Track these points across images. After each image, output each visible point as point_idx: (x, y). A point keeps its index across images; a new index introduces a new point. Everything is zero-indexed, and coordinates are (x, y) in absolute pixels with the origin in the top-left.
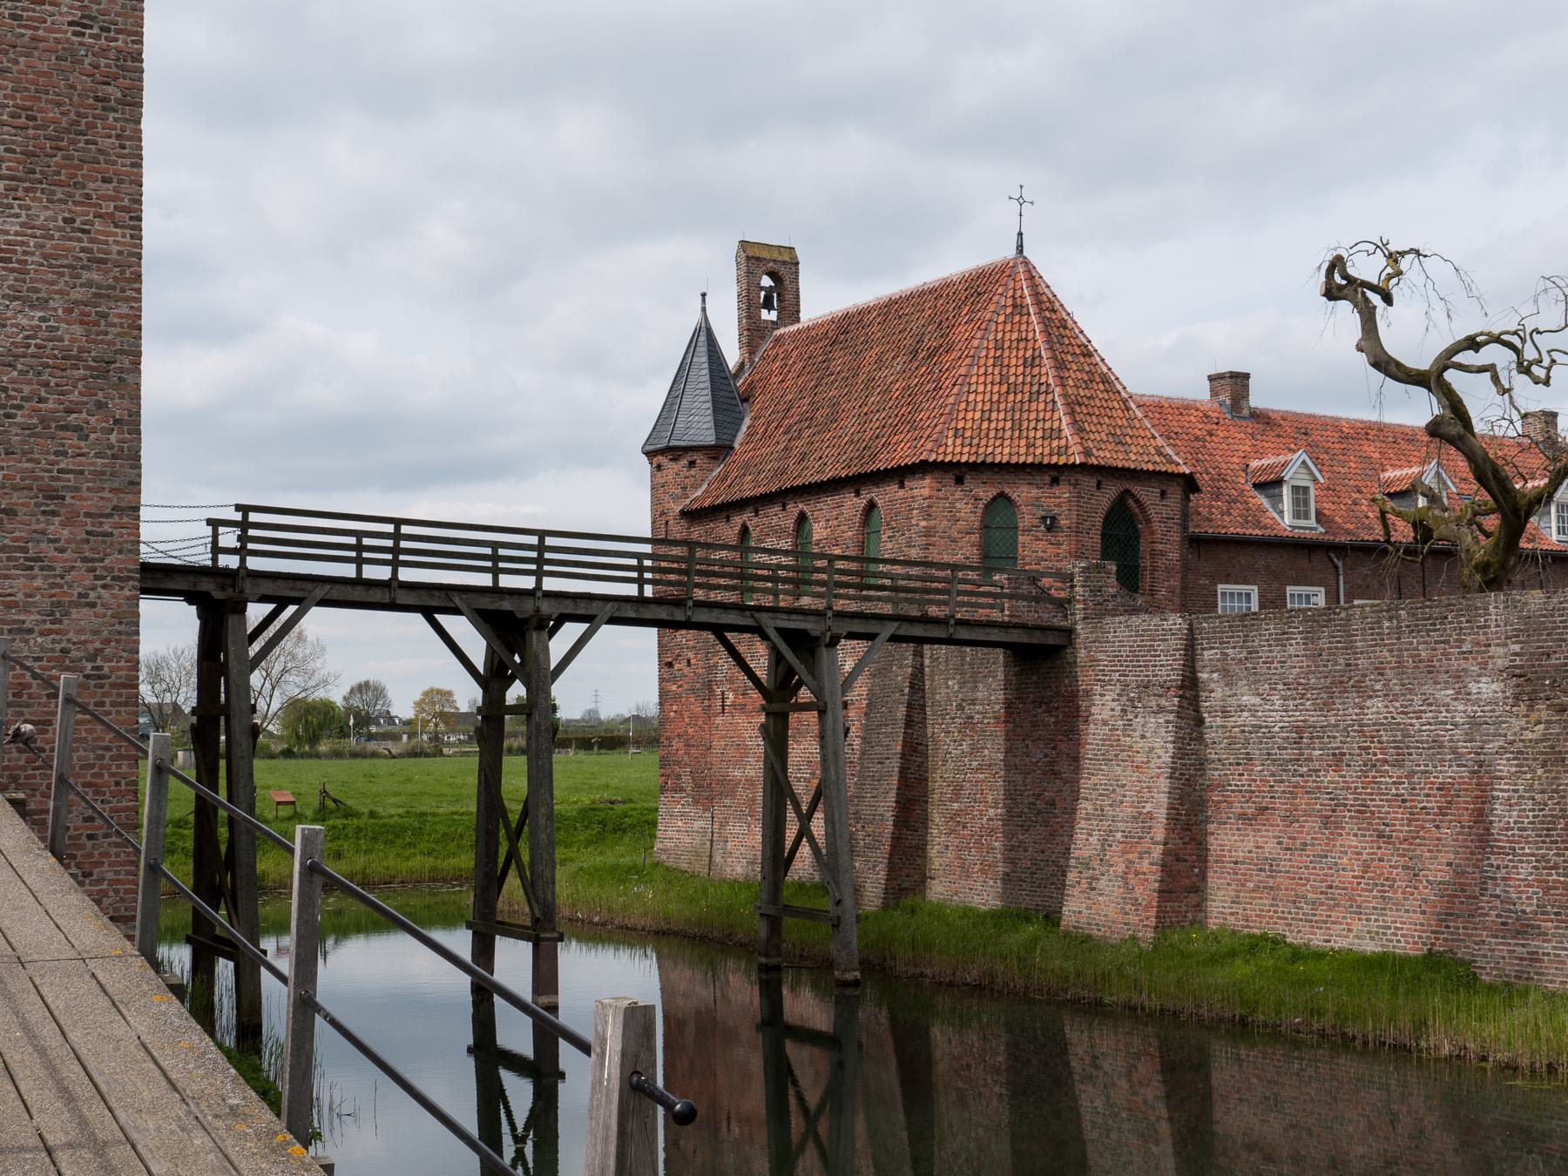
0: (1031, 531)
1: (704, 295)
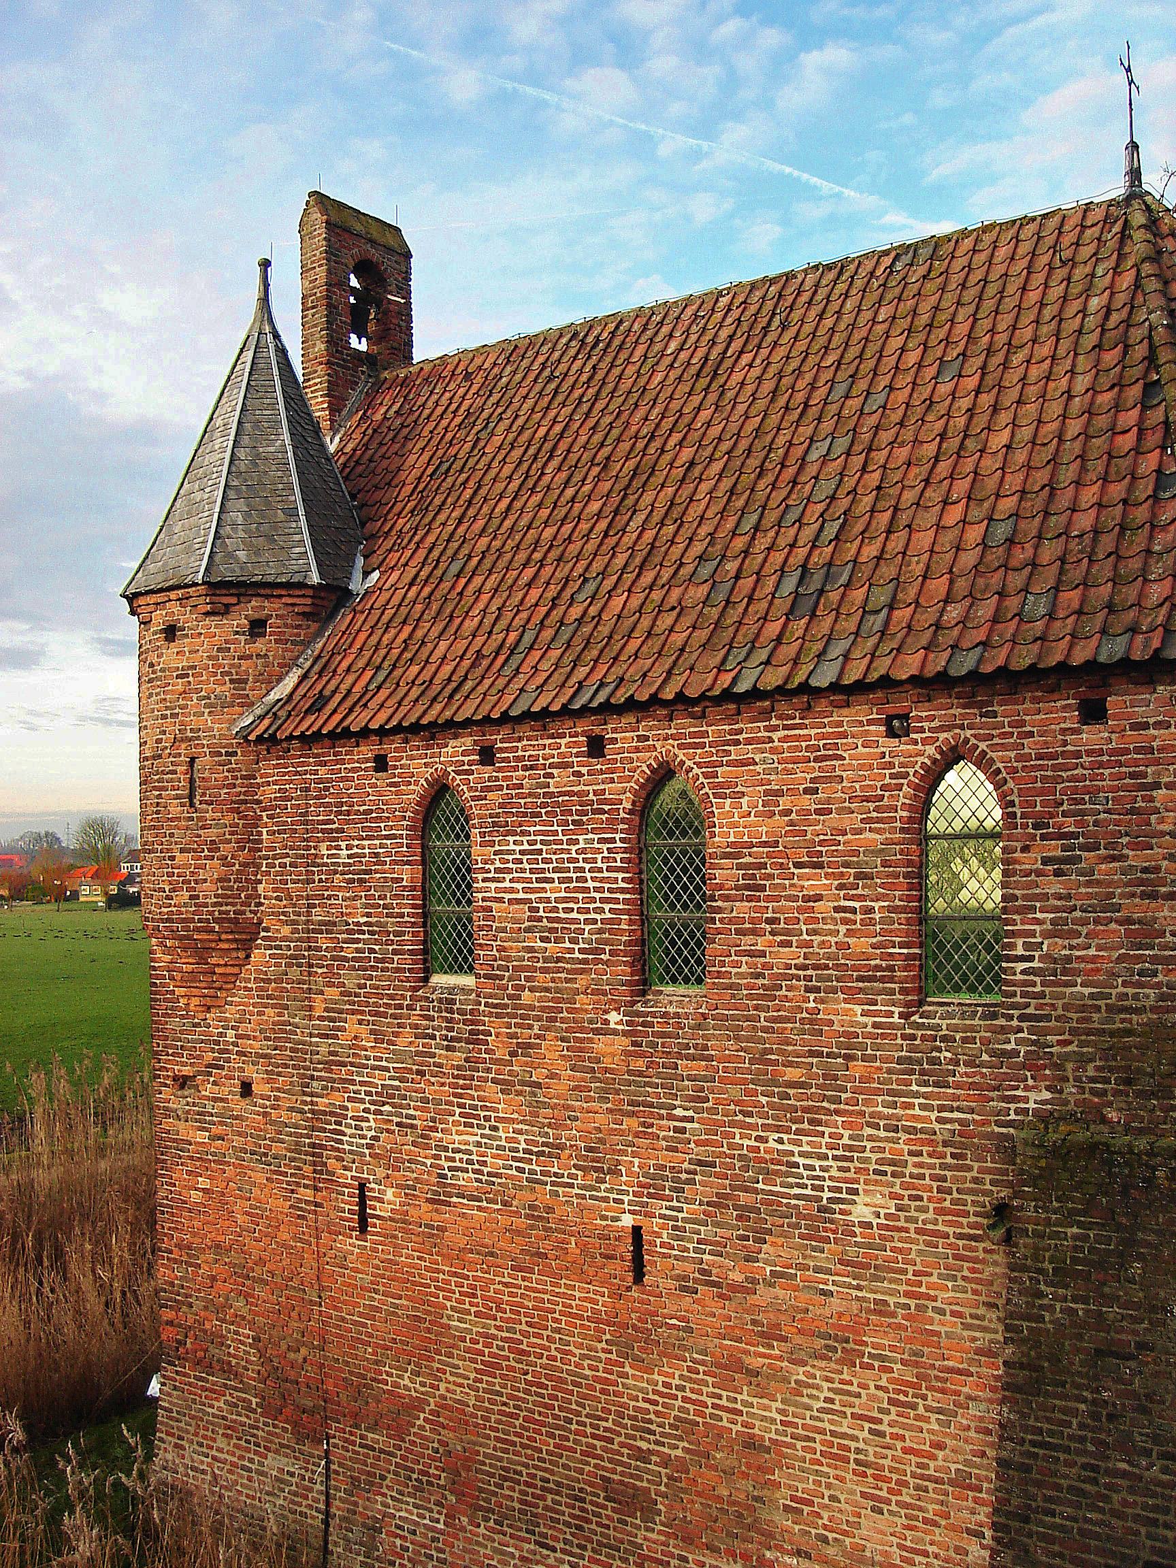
1: (265, 264)
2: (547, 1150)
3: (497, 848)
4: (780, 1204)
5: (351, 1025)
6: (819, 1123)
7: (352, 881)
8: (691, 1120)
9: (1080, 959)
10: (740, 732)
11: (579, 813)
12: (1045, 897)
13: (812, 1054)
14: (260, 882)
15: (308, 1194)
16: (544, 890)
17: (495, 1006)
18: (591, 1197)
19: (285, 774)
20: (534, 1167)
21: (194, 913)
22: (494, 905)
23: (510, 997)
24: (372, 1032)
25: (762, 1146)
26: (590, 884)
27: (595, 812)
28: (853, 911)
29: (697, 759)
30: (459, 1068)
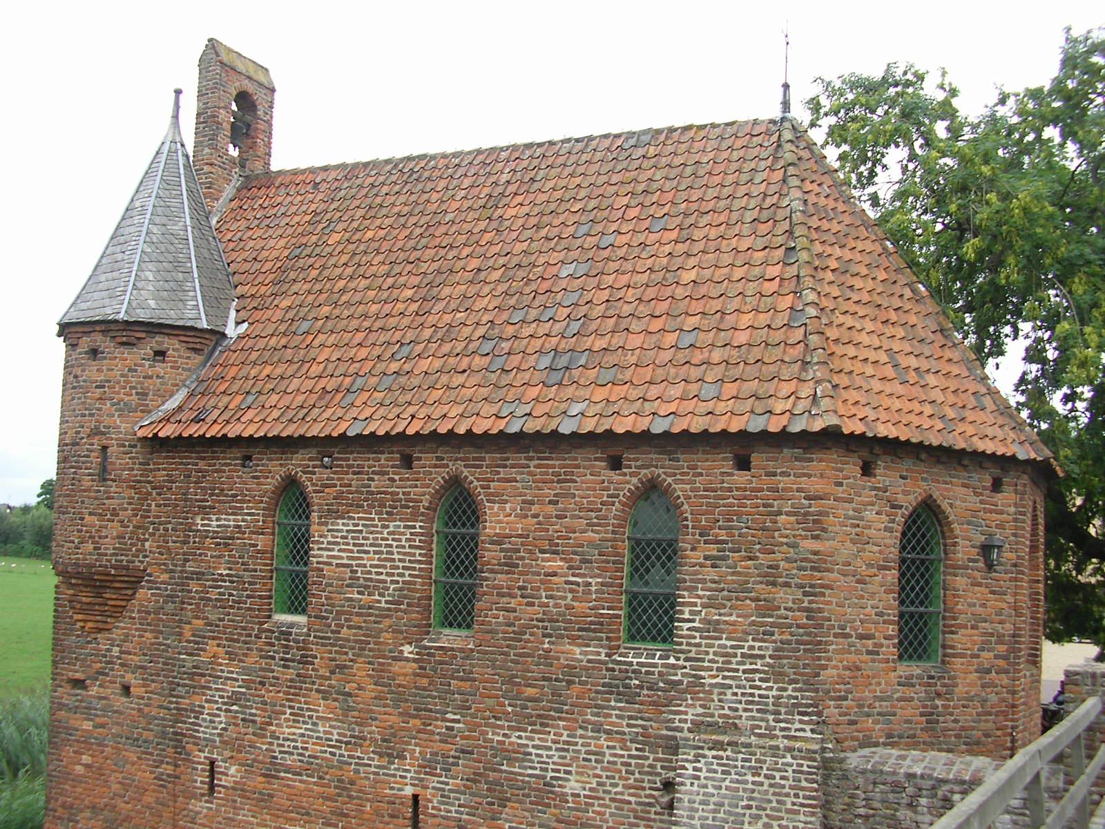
0: (967, 568)
2: (353, 740)
3: (330, 527)
4: (517, 780)
5: (211, 646)
6: (547, 725)
7: (219, 544)
8: (458, 721)
9: (726, 622)
10: (508, 459)
11: (390, 506)
12: (704, 581)
13: (544, 679)
14: (147, 540)
15: (170, 769)
16: (362, 559)
17: (321, 638)
18: (383, 774)
19: (172, 464)
20: (343, 752)
21: (96, 560)
22: (326, 567)
23: (333, 632)
24: (227, 653)
25: (507, 740)
26: (396, 556)
27: (402, 507)
28: (578, 584)
29: (477, 475)
30: (291, 680)
